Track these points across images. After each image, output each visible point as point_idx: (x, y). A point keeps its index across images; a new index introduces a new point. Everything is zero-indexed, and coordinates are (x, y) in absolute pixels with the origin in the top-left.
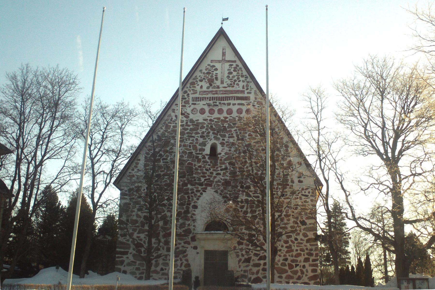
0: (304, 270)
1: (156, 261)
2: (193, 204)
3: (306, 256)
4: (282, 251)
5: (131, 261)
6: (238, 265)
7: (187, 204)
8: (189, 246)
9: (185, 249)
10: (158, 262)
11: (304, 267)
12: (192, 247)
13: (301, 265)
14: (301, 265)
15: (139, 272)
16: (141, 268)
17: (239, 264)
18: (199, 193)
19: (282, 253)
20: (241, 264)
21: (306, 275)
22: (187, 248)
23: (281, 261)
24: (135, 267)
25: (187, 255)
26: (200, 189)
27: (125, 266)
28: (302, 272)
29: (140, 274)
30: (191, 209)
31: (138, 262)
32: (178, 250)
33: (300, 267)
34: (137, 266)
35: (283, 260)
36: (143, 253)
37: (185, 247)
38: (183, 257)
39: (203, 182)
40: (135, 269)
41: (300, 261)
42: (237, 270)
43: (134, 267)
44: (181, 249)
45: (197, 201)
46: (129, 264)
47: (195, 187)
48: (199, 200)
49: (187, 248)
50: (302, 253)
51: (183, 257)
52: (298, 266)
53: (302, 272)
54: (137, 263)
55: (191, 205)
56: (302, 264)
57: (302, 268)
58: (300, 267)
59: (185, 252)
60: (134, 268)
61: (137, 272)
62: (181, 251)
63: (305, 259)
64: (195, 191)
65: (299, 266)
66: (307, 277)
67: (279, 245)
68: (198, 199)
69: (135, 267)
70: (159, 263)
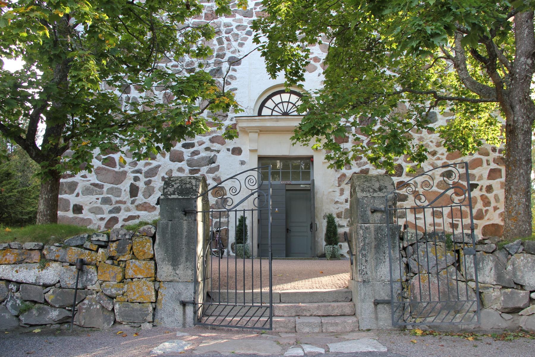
0: (491, 196)
1: (148, 183)
2: (228, 55)
3: (494, 166)
4: (438, 155)
5: (91, 184)
6: (338, 190)
7: (218, 56)
8: (223, 148)
9: (212, 154)
10: (151, 185)
11: (489, 189)
12: (228, 150)
13: (482, 186)
14: (482, 186)
15: (110, 208)
16: (114, 199)
17: (339, 185)
18: (244, 32)
19: (439, 159)
20: (343, 186)
21: (496, 209)
22: (218, 151)
23: (439, 179)
24: (101, 196)
25: (217, 168)
26: (245, 24)
27: (78, 195)
28: (487, 203)
29: (110, 212)
30: (225, 66)
31: (107, 186)
32: (196, 157)
33: (481, 189)
34: (105, 195)
35: (443, 175)
36: (118, 166)
37: (212, 151)
38: (208, 172)
39: (252, 9)
40: (100, 200)
41: (481, 178)
42: (336, 200)
43: (97, 196)
44: (203, 154)
45: (240, 49)
46: (87, 191)
47: (233, 21)
48: (244, 46)
49: (218, 151)
50: (484, 158)
51: (208, 172)
52: (476, 188)
53: (487, 203)
54: (105, 189)
55: (226, 58)
56: (485, 183)
57: (484, 192)
58: (481, 189)
59: (212, 161)
60: (98, 199)
61: (107, 208)
62: (203, 158)
63: (492, 171)
64: (234, 27)
65: (479, 187)
66: (498, 212)
67: (431, 142)
68: (241, 45)
69: (101, 196)
70: (153, 188)
